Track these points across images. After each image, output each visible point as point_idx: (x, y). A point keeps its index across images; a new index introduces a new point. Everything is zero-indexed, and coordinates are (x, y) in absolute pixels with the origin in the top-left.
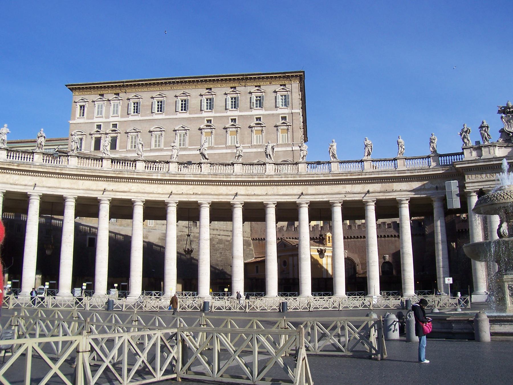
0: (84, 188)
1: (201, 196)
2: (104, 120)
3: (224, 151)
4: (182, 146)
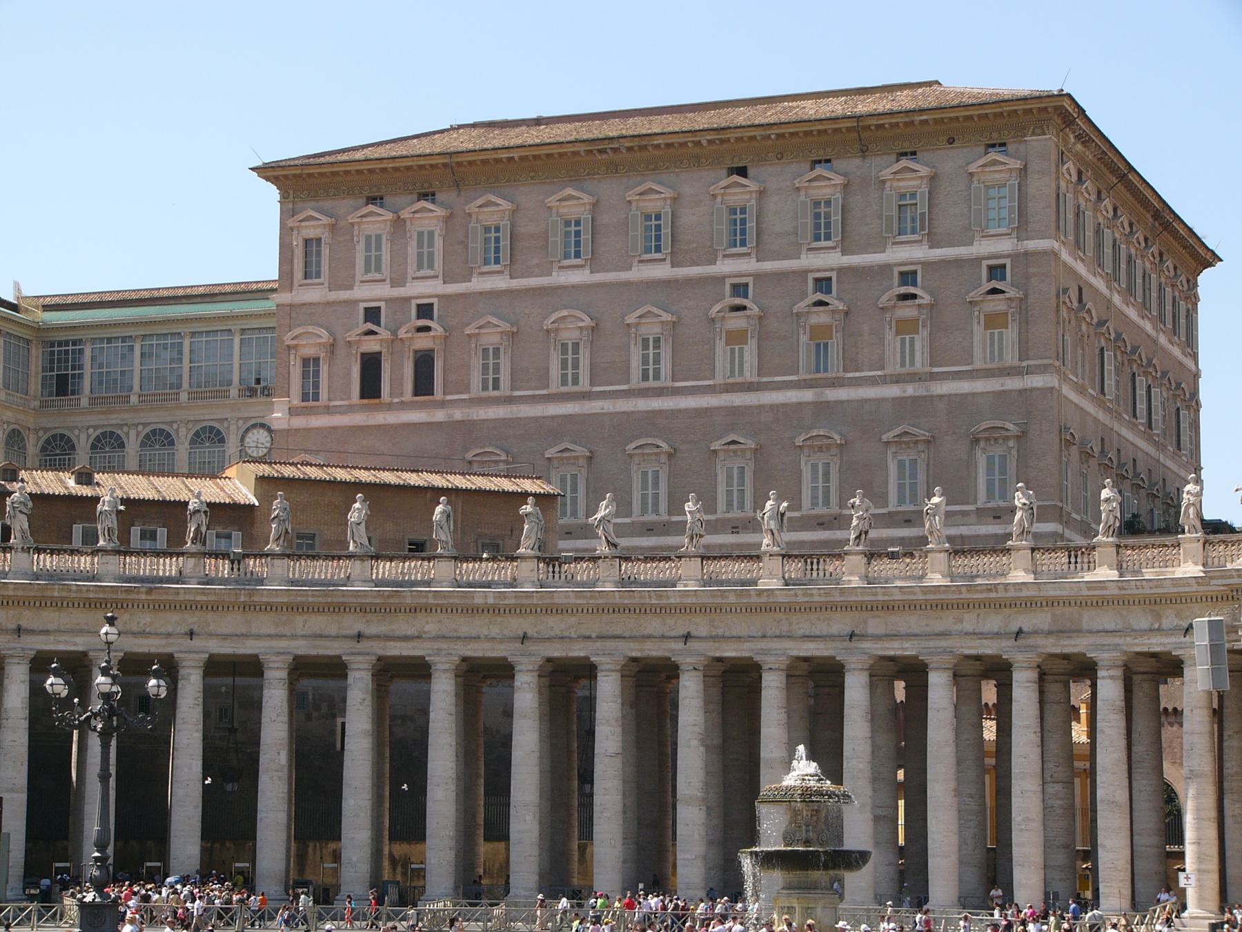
0: (307, 632)
1: (598, 644)
2: (385, 291)
3: (792, 396)
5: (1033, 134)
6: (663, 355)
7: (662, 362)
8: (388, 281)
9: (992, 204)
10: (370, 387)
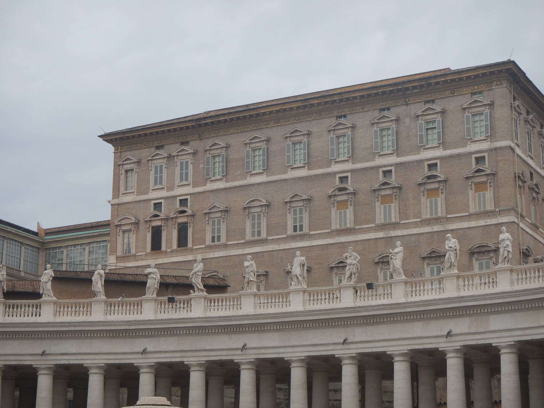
4: (298, 232)
5: (497, 85)
6: (304, 218)
7: (304, 221)
8: (165, 189)
9: (477, 124)
10: (156, 245)
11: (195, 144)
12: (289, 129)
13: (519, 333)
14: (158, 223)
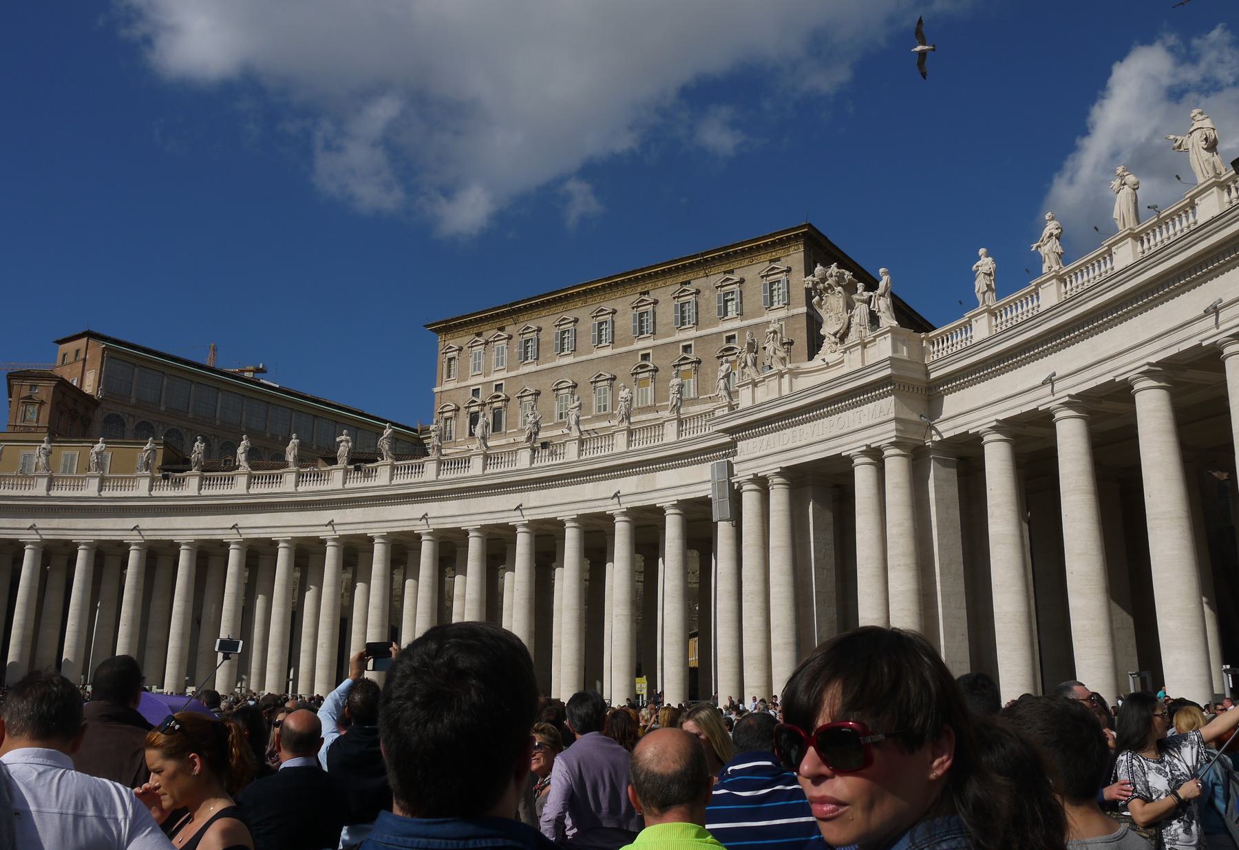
2: (481, 379)
11: (510, 329)
12: (594, 307)
13: (683, 490)
14: (476, 409)
